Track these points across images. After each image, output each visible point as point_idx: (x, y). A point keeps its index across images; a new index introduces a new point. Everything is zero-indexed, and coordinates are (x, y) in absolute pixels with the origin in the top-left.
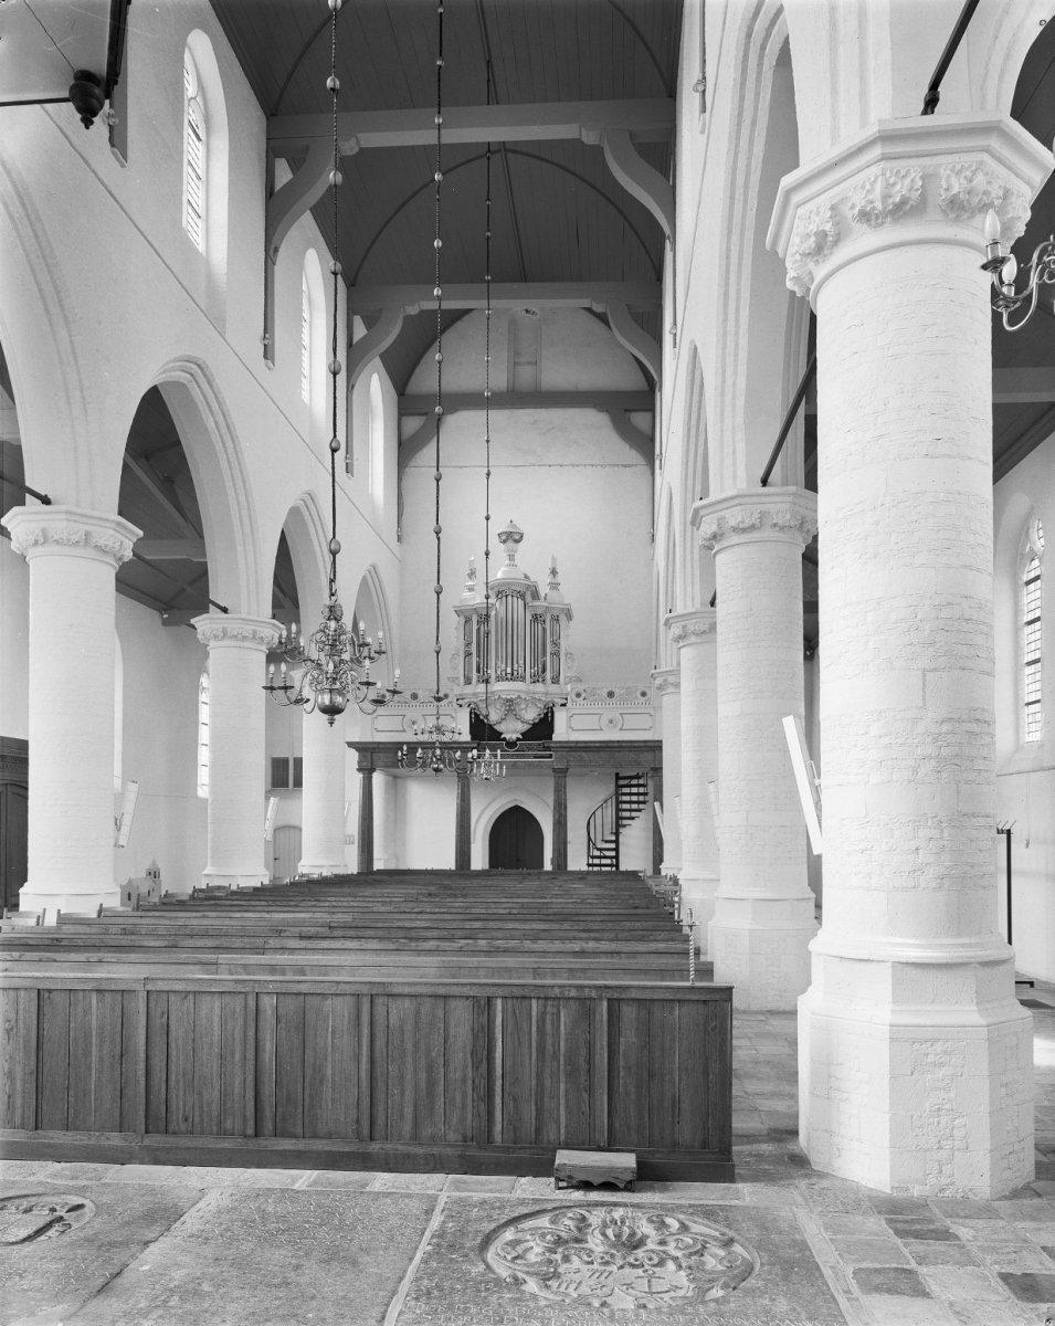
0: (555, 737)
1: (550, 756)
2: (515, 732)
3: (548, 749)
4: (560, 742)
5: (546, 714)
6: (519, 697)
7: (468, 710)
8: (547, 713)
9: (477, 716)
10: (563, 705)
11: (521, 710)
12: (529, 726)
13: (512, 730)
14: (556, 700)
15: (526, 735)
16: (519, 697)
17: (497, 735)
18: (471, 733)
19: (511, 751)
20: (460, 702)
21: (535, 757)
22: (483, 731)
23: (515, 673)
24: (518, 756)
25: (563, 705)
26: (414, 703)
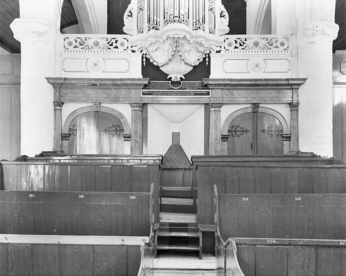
0: (211, 77)
1: (208, 94)
2: (178, 73)
3: (206, 86)
4: (217, 80)
5: (204, 59)
6: (185, 38)
7: (141, 54)
8: (206, 57)
9: (148, 60)
10: (219, 52)
11: (186, 51)
12: (191, 68)
13: (176, 71)
14: (213, 47)
15: (188, 76)
16: (185, 38)
17: (164, 76)
18: (142, 74)
19: (176, 89)
20: (134, 49)
21: (195, 94)
22: (150, 69)
23: (182, 17)
24: (181, 94)
25: (219, 52)
26: (96, 49)
